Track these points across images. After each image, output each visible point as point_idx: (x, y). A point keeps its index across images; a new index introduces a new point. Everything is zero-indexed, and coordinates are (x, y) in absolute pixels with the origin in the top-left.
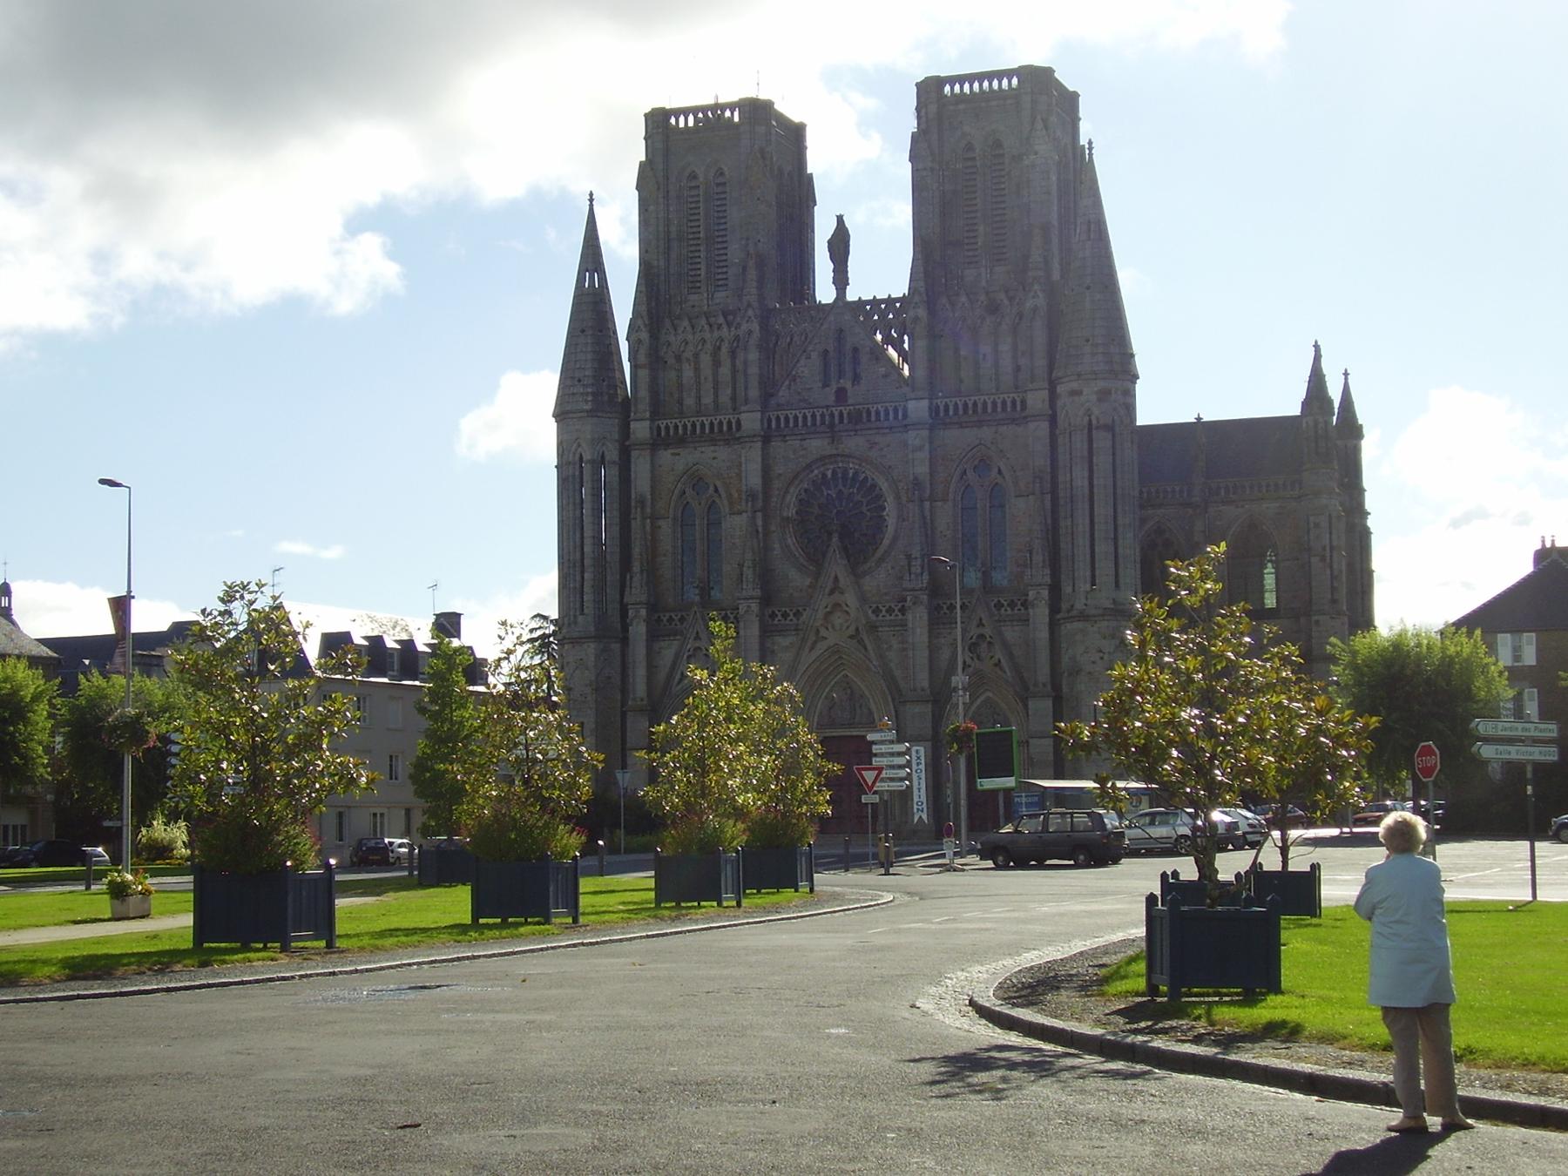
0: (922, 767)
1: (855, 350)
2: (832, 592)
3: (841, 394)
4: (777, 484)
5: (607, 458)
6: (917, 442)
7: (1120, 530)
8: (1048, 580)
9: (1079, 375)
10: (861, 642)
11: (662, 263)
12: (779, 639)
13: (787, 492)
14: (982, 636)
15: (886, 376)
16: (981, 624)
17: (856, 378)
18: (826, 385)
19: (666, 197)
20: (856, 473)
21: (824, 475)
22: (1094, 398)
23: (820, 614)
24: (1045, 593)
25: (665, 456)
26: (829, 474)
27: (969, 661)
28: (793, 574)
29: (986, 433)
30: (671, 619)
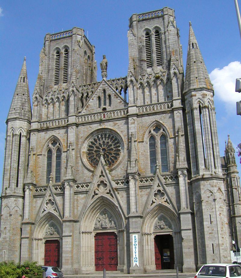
0: (137, 243)
1: (110, 96)
2: (100, 176)
3: (104, 109)
4: (80, 140)
5: (22, 134)
6: (132, 121)
7: (214, 146)
8: (186, 166)
9: (194, 89)
10: (111, 195)
11: (46, 76)
12: (80, 195)
13: (84, 142)
14: (159, 191)
15: (121, 102)
16: (159, 186)
17: (110, 105)
18: (99, 107)
19: (49, 58)
20: (109, 136)
21: (98, 137)
22: (201, 97)
23: (96, 186)
24: (185, 172)
25: (43, 134)
26: (100, 136)
27: (154, 200)
28: (86, 171)
29: (157, 118)
30: (41, 190)
